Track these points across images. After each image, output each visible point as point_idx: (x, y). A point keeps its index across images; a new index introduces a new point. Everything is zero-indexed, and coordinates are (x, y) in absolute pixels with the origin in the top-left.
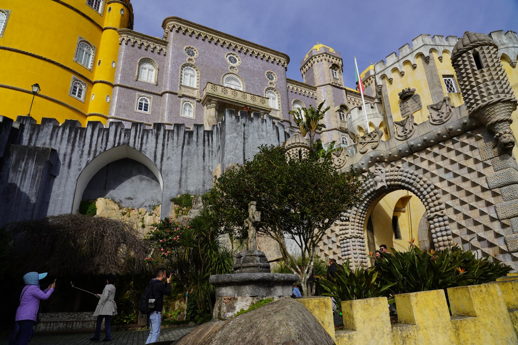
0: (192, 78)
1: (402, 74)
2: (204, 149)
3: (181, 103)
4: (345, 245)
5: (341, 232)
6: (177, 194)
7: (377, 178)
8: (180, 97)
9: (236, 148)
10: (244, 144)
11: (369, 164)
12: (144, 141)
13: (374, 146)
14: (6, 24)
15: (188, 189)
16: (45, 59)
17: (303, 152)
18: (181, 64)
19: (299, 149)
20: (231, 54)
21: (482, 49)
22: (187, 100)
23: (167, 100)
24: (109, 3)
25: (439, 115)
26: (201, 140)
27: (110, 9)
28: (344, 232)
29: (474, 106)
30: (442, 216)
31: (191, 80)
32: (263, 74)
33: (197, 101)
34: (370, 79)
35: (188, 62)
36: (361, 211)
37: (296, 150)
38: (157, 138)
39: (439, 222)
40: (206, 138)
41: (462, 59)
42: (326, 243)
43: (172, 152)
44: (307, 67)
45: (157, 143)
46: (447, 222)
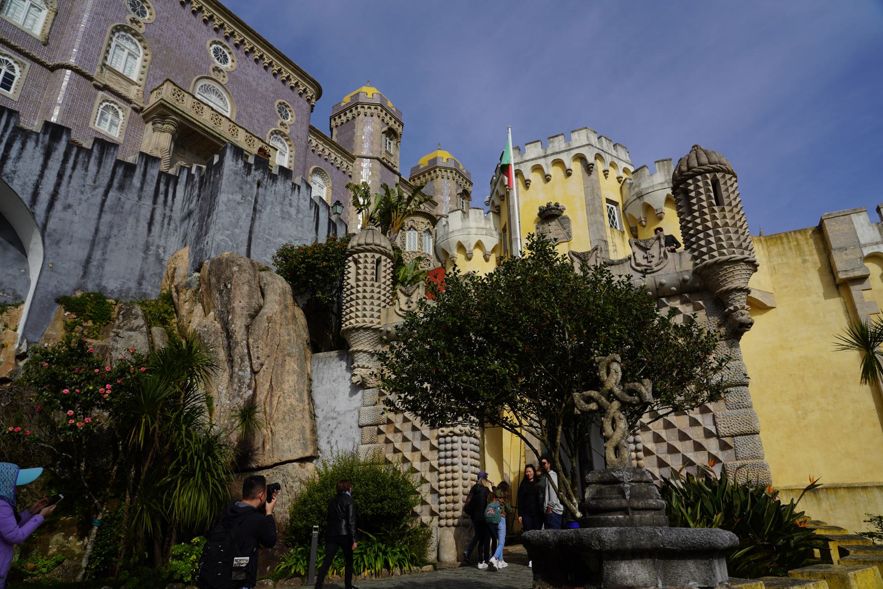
0: (130, 59)
1: (547, 179)
2: (154, 210)
3: (98, 101)
6: (75, 290)
8: (97, 87)
9: (236, 225)
10: (253, 220)
12: (14, 153)
15: (104, 283)
17: (383, 263)
18: (113, 21)
19: (377, 256)
20: (220, 43)
21: (724, 177)
22: (112, 99)
23: (65, 84)
25: (647, 258)
26: (150, 189)
29: (706, 257)
31: (129, 62)
32: (273, 103)
33: (134, 109)
34: (435, 172)
35: (129, 24)
37: (373, 257)
38: (47, 155)
40: (162, 187)
41: (694, 183)
42: (410, 437)
43: (78, 195)
44: (344, 118)
45: (45, 166)
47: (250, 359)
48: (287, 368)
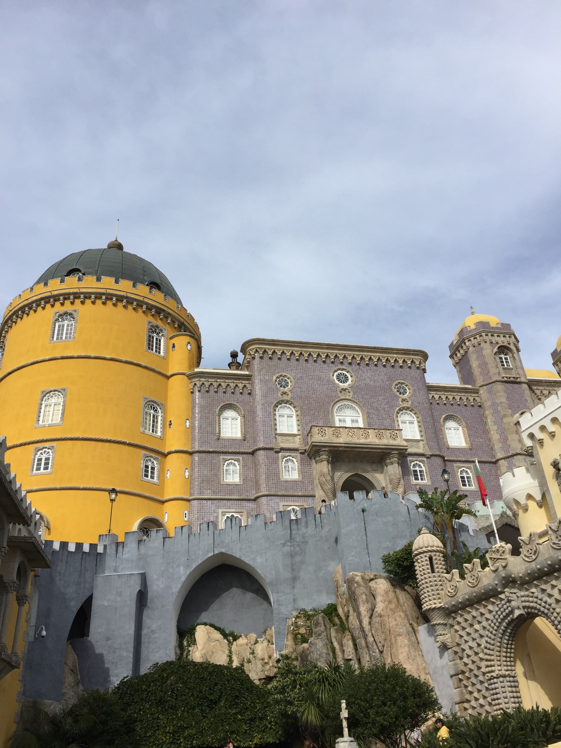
0: (289, 419)
3: (280, 461)
4: (493, 686)
5: (487, 669)
7: (513, 604)
8: (277, 452)
11: (504, 584)
13: (504, 564)
14: (64, 406)
17: (434, 558)
18: (272, 403)
20: (339, 369)
22: (287, 454)
24: (171, 338)
27: (174, 346)
28: (490, 669)
47: (377, 645)
48: (399, 644)
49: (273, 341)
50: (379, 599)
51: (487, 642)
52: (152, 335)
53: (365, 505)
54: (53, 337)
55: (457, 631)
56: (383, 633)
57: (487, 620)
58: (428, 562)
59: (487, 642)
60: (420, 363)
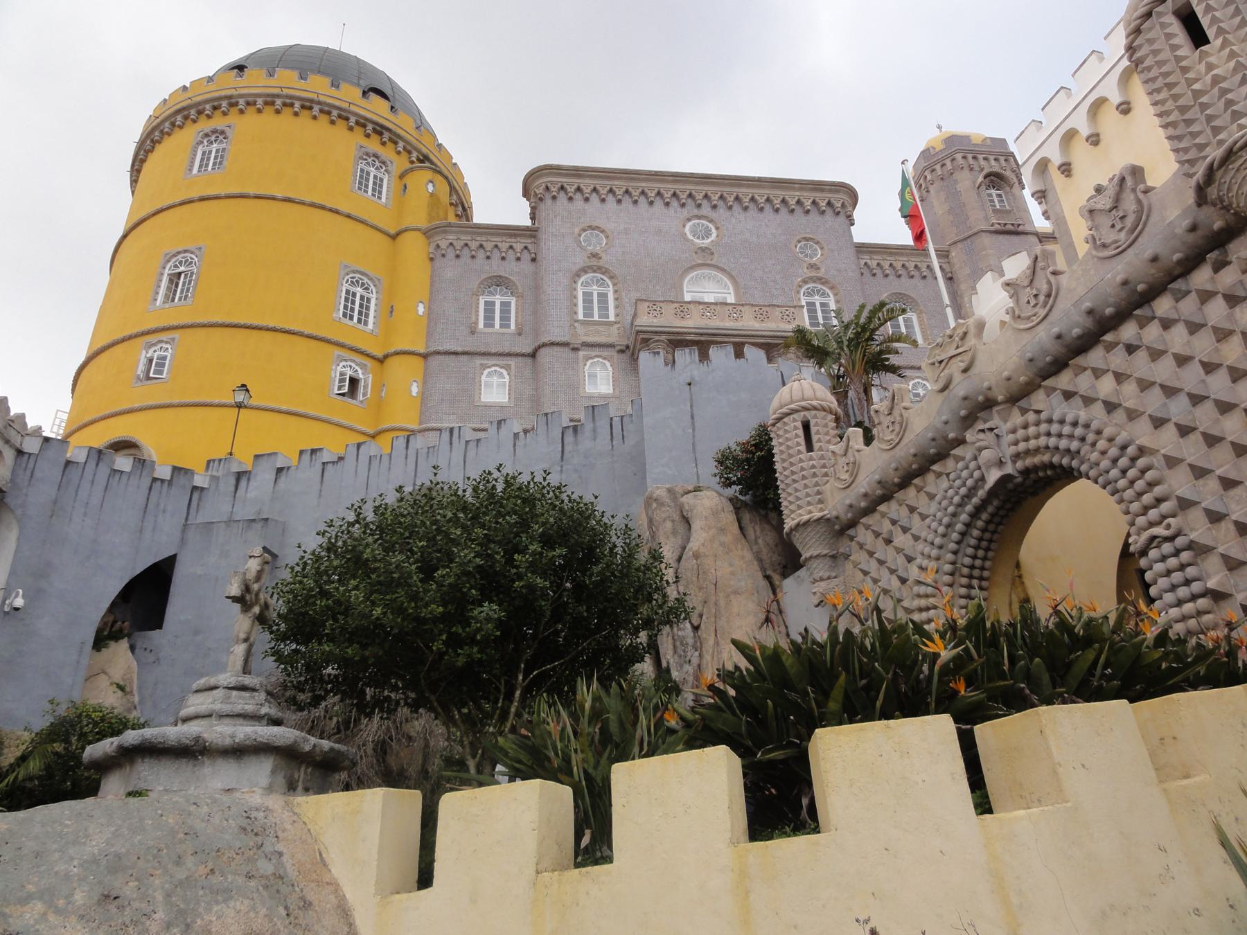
3: (581, 364)
7: (986, 454)
8: (575, 349)
11: (965, 418)
13: (963, 365)
16: (273, 330)
19: (799, 417)
22: (594, 354)
30: (1171, 539)
33: (622, 351)
36: (967, 561)
39: (1163, 559)
46: (1185, 556)
49: (577, 169)
50: (696, 525)
51: (921, 568)
52: (367, 168)
53: (696, 373)
54: (191, 170)
55: (856, 565)
56: (700, 588)
57: (923, 517)
58: (801, 432)
59: (921, 568)
60: (843, 205)
